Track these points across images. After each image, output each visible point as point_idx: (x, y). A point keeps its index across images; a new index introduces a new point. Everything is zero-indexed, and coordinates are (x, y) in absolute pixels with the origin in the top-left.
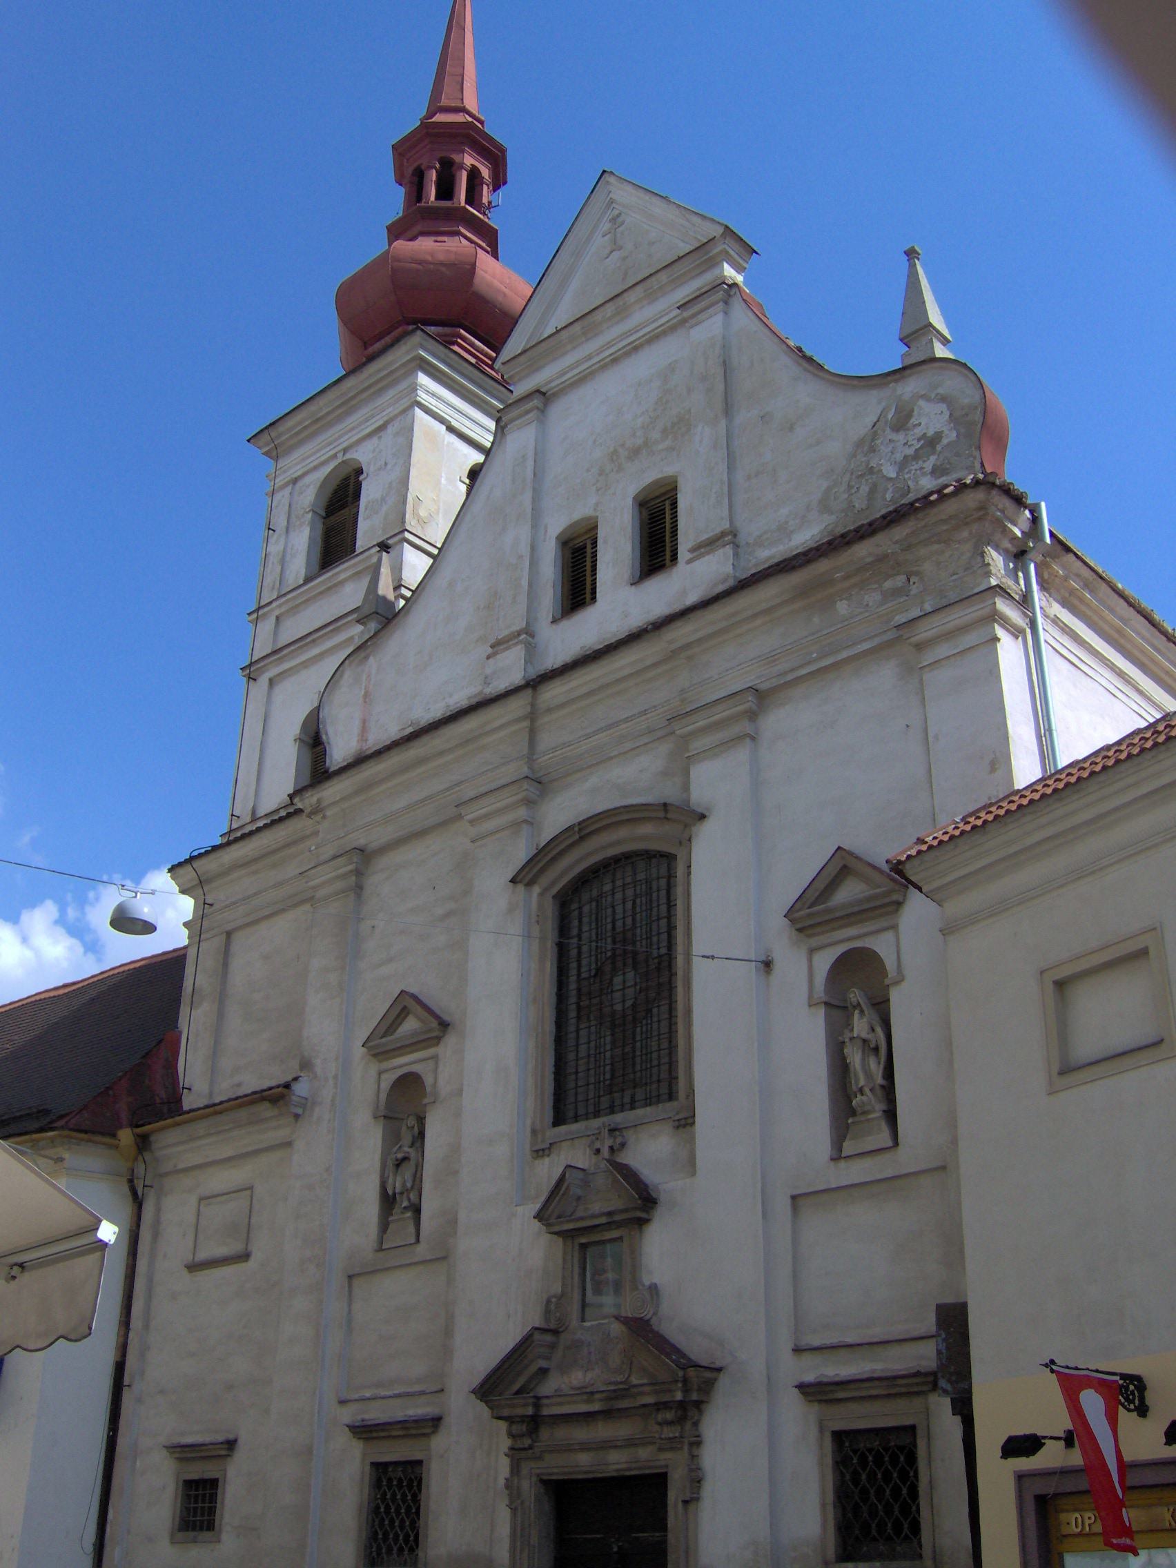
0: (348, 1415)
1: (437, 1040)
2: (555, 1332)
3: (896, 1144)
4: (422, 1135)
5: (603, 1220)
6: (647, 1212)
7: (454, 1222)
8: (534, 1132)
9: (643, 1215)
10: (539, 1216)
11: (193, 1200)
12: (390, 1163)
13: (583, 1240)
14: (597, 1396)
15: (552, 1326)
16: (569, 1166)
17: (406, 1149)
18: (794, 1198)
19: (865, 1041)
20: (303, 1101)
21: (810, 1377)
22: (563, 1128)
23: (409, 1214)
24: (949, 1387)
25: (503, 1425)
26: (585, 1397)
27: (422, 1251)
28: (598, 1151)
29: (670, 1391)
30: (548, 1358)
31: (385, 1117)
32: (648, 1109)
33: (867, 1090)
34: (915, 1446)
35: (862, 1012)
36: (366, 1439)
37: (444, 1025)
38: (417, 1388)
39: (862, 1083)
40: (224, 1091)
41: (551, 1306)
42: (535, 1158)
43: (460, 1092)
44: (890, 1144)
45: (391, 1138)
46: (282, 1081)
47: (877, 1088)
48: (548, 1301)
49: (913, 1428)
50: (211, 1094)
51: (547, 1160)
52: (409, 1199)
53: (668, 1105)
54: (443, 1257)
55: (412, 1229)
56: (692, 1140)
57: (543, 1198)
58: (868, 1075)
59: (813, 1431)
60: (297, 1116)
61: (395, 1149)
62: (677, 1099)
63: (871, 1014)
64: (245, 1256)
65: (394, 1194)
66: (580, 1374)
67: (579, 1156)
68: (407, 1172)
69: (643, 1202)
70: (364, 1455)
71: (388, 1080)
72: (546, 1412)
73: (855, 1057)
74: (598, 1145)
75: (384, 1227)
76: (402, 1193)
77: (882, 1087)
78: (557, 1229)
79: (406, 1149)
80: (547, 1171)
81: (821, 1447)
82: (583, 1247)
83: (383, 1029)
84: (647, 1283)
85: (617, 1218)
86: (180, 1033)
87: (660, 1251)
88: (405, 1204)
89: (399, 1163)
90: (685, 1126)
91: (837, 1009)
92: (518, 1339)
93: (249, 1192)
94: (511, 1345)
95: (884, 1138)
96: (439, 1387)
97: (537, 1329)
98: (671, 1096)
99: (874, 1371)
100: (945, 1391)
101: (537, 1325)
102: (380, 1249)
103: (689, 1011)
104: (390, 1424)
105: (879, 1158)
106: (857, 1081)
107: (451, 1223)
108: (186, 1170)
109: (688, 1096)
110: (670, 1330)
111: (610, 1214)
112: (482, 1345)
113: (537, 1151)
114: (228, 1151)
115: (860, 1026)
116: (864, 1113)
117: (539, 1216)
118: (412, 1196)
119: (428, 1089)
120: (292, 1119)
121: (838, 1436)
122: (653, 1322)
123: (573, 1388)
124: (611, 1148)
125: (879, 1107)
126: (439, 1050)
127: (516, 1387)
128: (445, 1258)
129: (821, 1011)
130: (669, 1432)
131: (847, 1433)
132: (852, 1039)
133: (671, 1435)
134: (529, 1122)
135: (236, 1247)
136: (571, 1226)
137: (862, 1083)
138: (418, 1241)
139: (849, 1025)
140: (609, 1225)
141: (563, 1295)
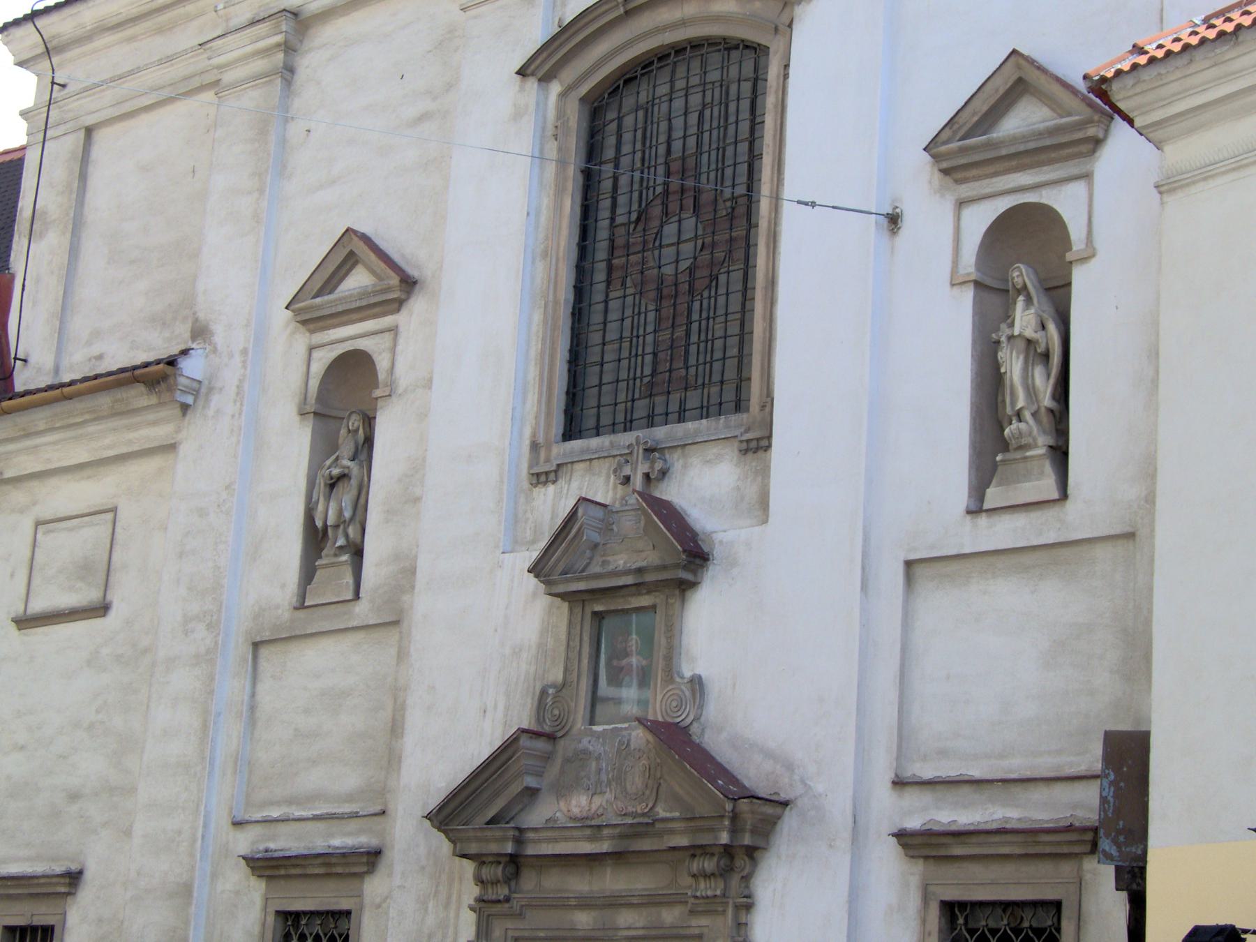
2: (551, 737)
3: (1064, 496)
4: (369, 441)
5: (629, 580)
6: (695, 573)
7: (412, 571)
8: (535, 446)
9: (688, 576)
10: (536, 569)
11: (27, 524)
12: (321, 482)
13: (599, 608)
14: (606, 832)
15: (547, 729)
16: (583, 500)
17: (346, 462)
18: (909, 564)
19: (1029, 342)
20: (195, 385)
21: (914, 823)
22: (576, 444)
23: (345, 558)
24: (1114, 851)
25: (469, 867)
26: (588, 832)
27: (363, 611)
28: (627, 480)
29: (711, 830)
30: (539, 775)
31: (315, 413)
32: (704, 421)
33: (1027, 415)
34: (1059, 930)
35: (1029, 300)
36: (270, 878)
38: (347, 808)
39: (1020, 403)
40: (76, 366)
41: (548, 699)
42: (534, 485)
43: (428, 384)
44: (1056, 495)
45: (324, 447)
46: (163, 354)
47: (1043, 410)
48: (544, 692)
49: (1058, 905)
50: (57, 370)
51: (551, 488)
52: (347, 536)
53: (734, 418)
54: (393, 622)
55: (349, 579)
56: (765, 472)
57: (543, 544)
58: (1031, 392)
59: (914, 901)
60: (185, 408)
61: (328, 463)
62: (747, 410)
63: (1041, 304)
64: (101, 609)
65: (325, 527)
66: (584, 800)
67: (598, 485)
68: (346, 496)
69: (690, 557)
71: (322, 360)
72: (530, 850)
73: (1013, 365)
74: (627, 471)
75: (308, 573)
76: (336, 527)
77: (1051, 411)
78: (561, 588)
79: (346, 462)
80: (552, 505)
81: (924, 922)
82: (599, 616)
84: (688, 674)
85: (650, 578)
86: (13, 277)
87: (711, 630)
88: (341, 542)
89: (333, 484)
90: (756, 450)
91: (992, 295)
92: (498, 743)
93: (110, 516)
94: (486, 753)
95: (1046, 485)
96: (378, 808)
97: (524, 731)
98: (739, 405)
99: (1006, 820)
100: (1108, 857)
101: (525, 725)
102: (301, 606)
103: (772, 283)
104: (305, 857)
105: (1036, 516)
106: (1013, 403)
107: (407, 574)
108: (17, 480)
109: (763, 407)
110: (716, 743)
111: (640, 571)
112: (442, 753)
113: (538, 475)
114: (81, 454)
115: (1024, 320)
116: (1020, 448)
117: (536, 569)
118: (351, 531)
119: (382, 376)
120: (178, 411)
121: (951, 909)
122: (695, 729)
123: (574, 819)
124: (647, 476)
125: (1042, 442)
126: (401, 318)
127: (491, 814)
128: (396, 623)
129: (968, 294)
130: (706, 888)
131: (962, 905)
132: (1011, 338)
133: (709, 893)
134: (528, 432)
135: (90, 595)
136: (582, 586)
137: (1020, 403)
138: (357, 596)
139: (1008, 318)
140: (639, 588)
141: (564, 684)
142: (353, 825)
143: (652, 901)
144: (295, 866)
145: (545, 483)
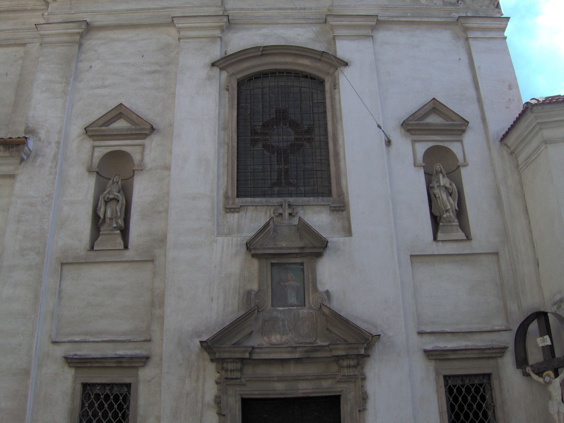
0: (60, 351)
1: (144, 136)
20: (29, 152)
36: (77, 368)
37: (153, 129)
38: (128, 338)
54: (149, 259)
60: (22, 160)
70: (75, 378)
83: (101, 122)
96: (148, 338)
104: (102, 358)
142: (131, 345)
143: (318, 378)
144: (97, 362)
145: (233, 212)
